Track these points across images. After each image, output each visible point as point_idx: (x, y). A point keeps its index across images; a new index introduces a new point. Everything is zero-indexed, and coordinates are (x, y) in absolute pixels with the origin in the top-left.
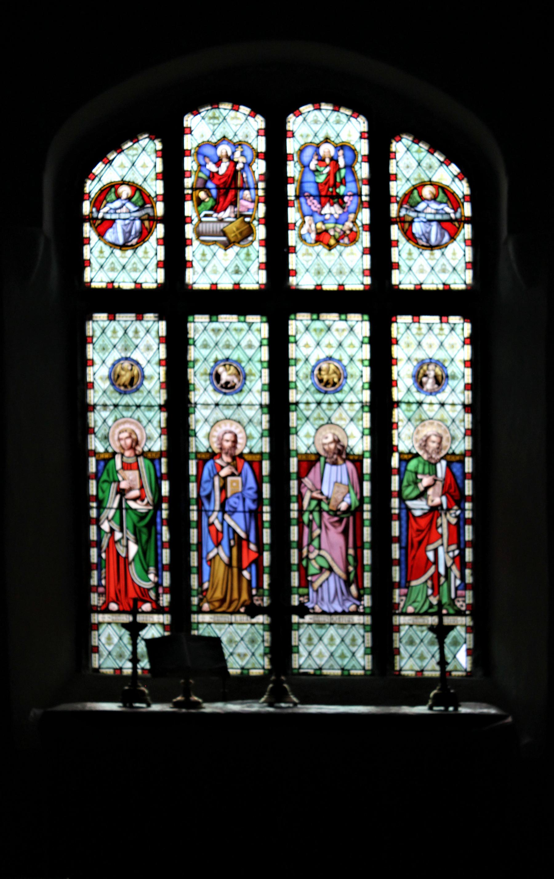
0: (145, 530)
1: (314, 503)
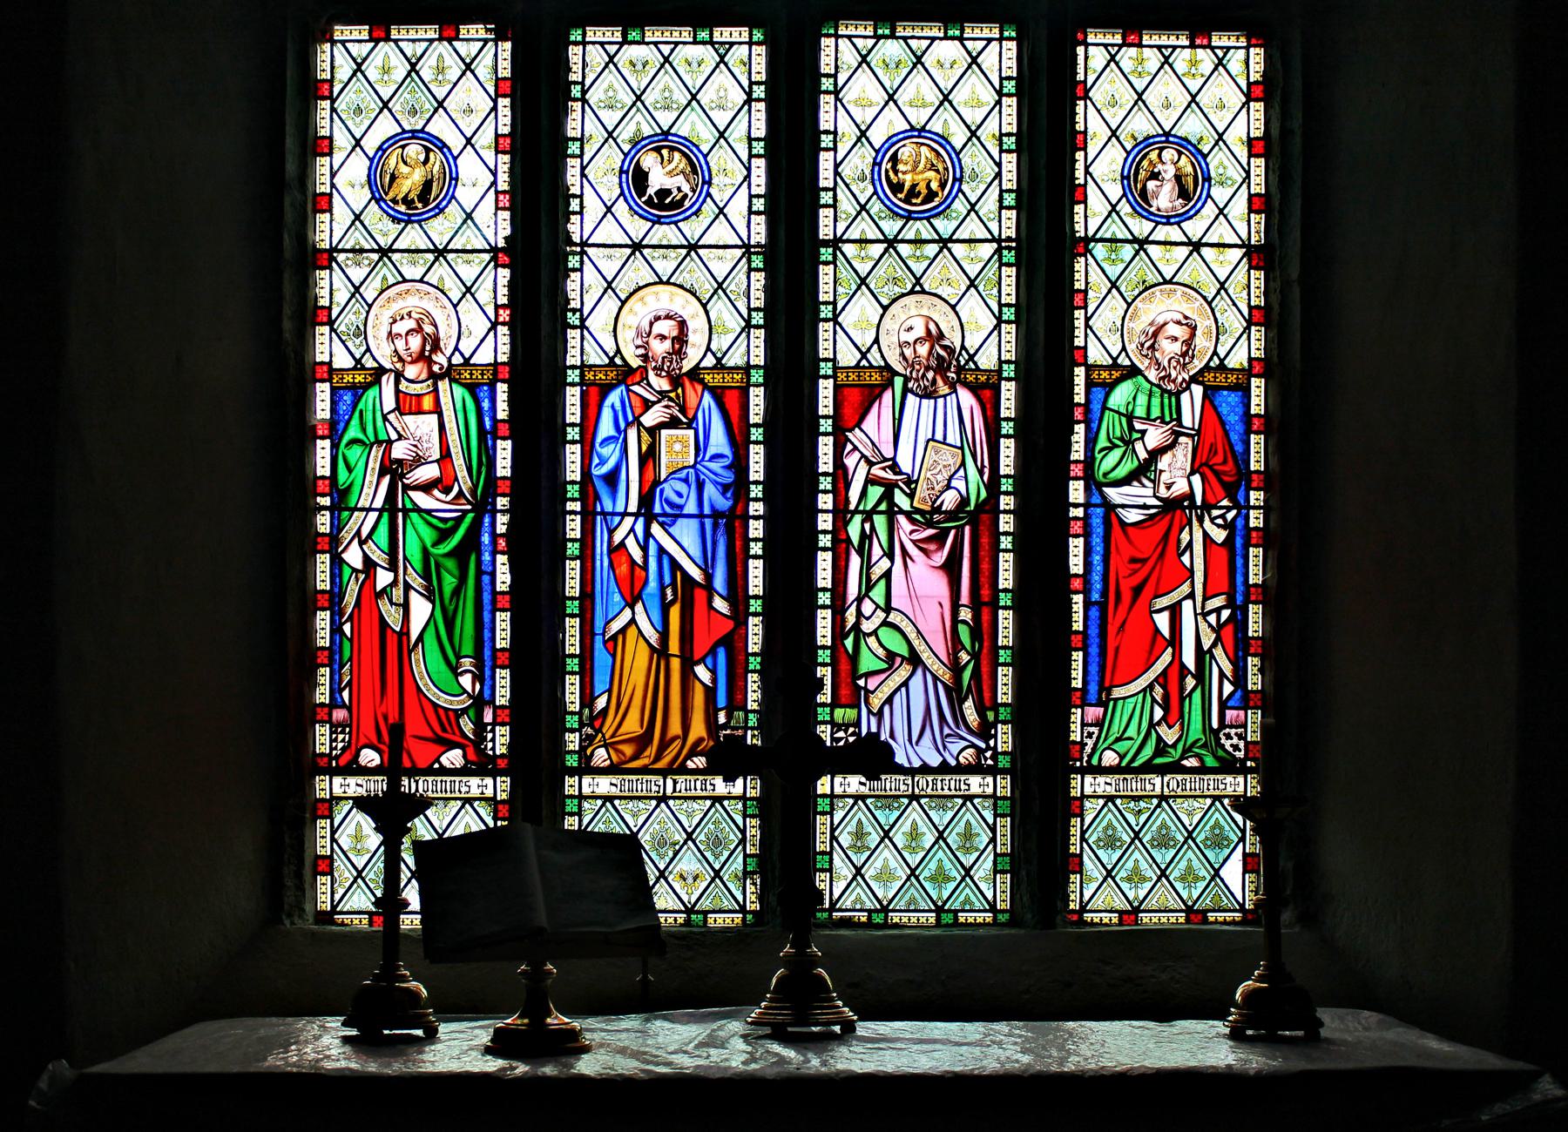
0: (450, 564)
1: (875, 492)
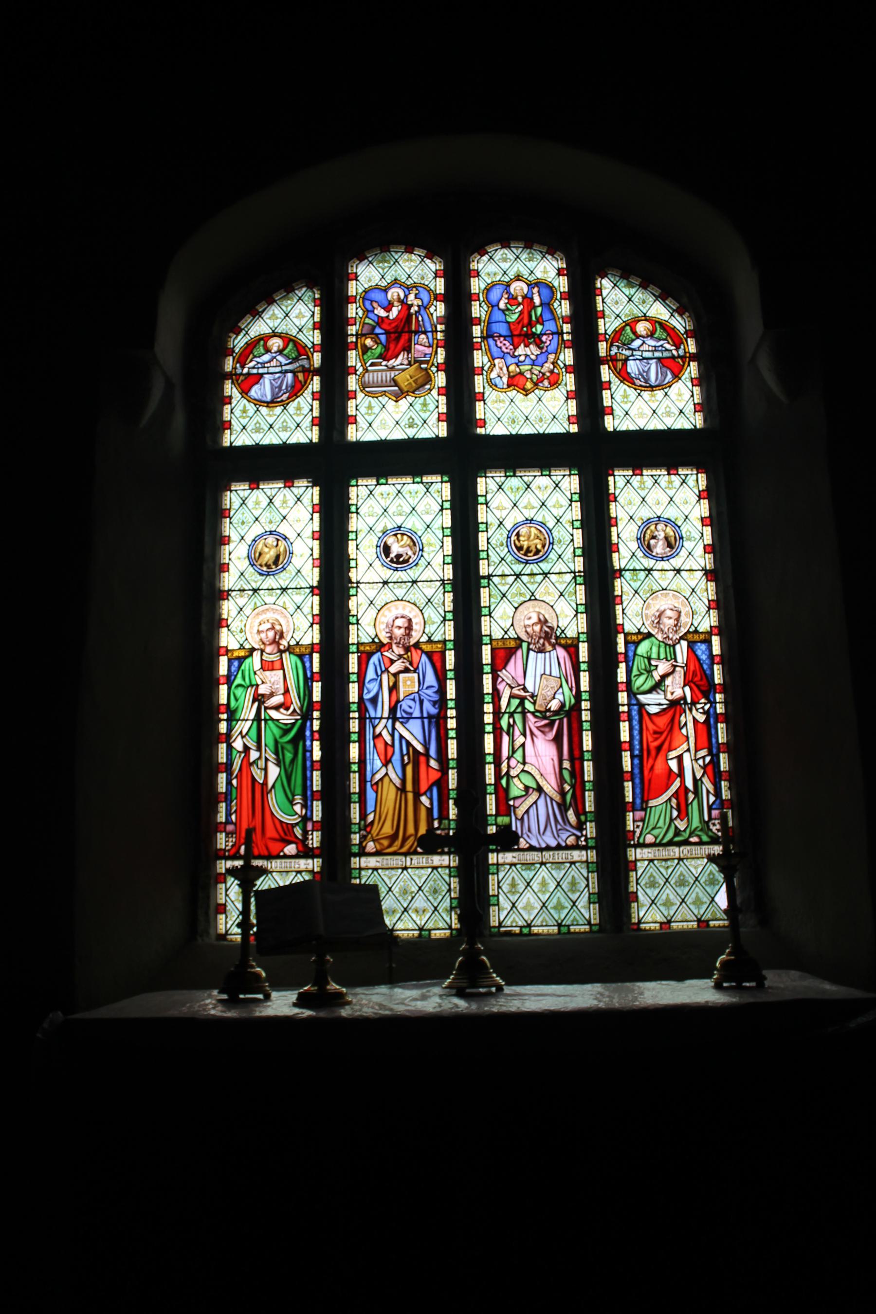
0: (289, 747)
1: (516, 702)
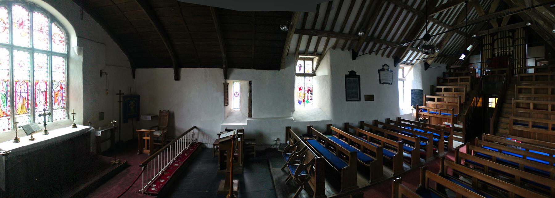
0: (4, 98)
